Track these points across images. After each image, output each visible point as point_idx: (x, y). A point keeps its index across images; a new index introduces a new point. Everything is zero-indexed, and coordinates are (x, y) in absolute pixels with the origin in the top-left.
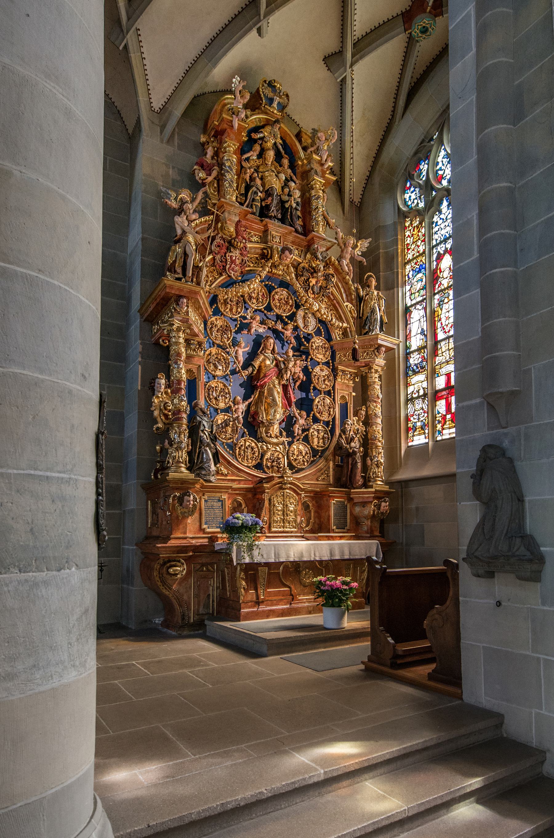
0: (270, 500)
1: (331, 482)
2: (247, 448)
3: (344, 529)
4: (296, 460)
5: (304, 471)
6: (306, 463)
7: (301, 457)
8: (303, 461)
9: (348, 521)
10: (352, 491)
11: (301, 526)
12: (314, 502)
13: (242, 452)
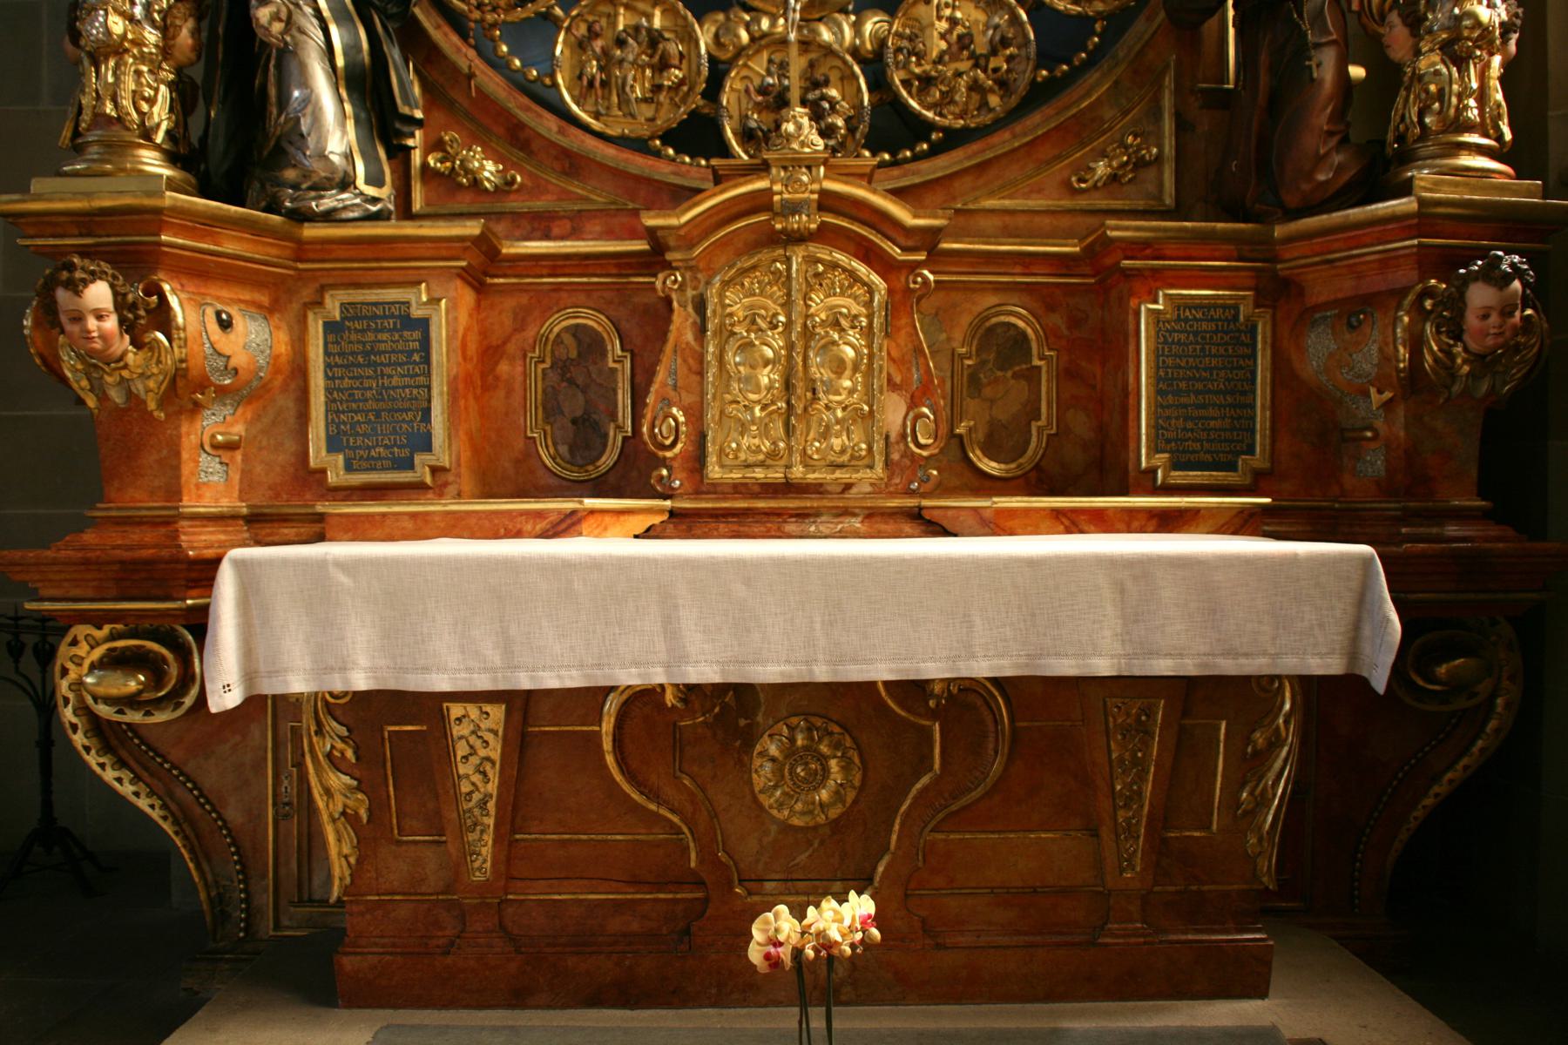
0: (700, 305)
1: (1169, 200)
2: (621, 43)
3: (1231, 467)
4: (927, 81)
5: (975, 147)
6: (994, 100)
7: (964, 66)
8: (975, 86)
9: (1262, 417)
10: (1279, 231)
11: (907, 453)
12: (1057, 320)
13: (593, 67)
